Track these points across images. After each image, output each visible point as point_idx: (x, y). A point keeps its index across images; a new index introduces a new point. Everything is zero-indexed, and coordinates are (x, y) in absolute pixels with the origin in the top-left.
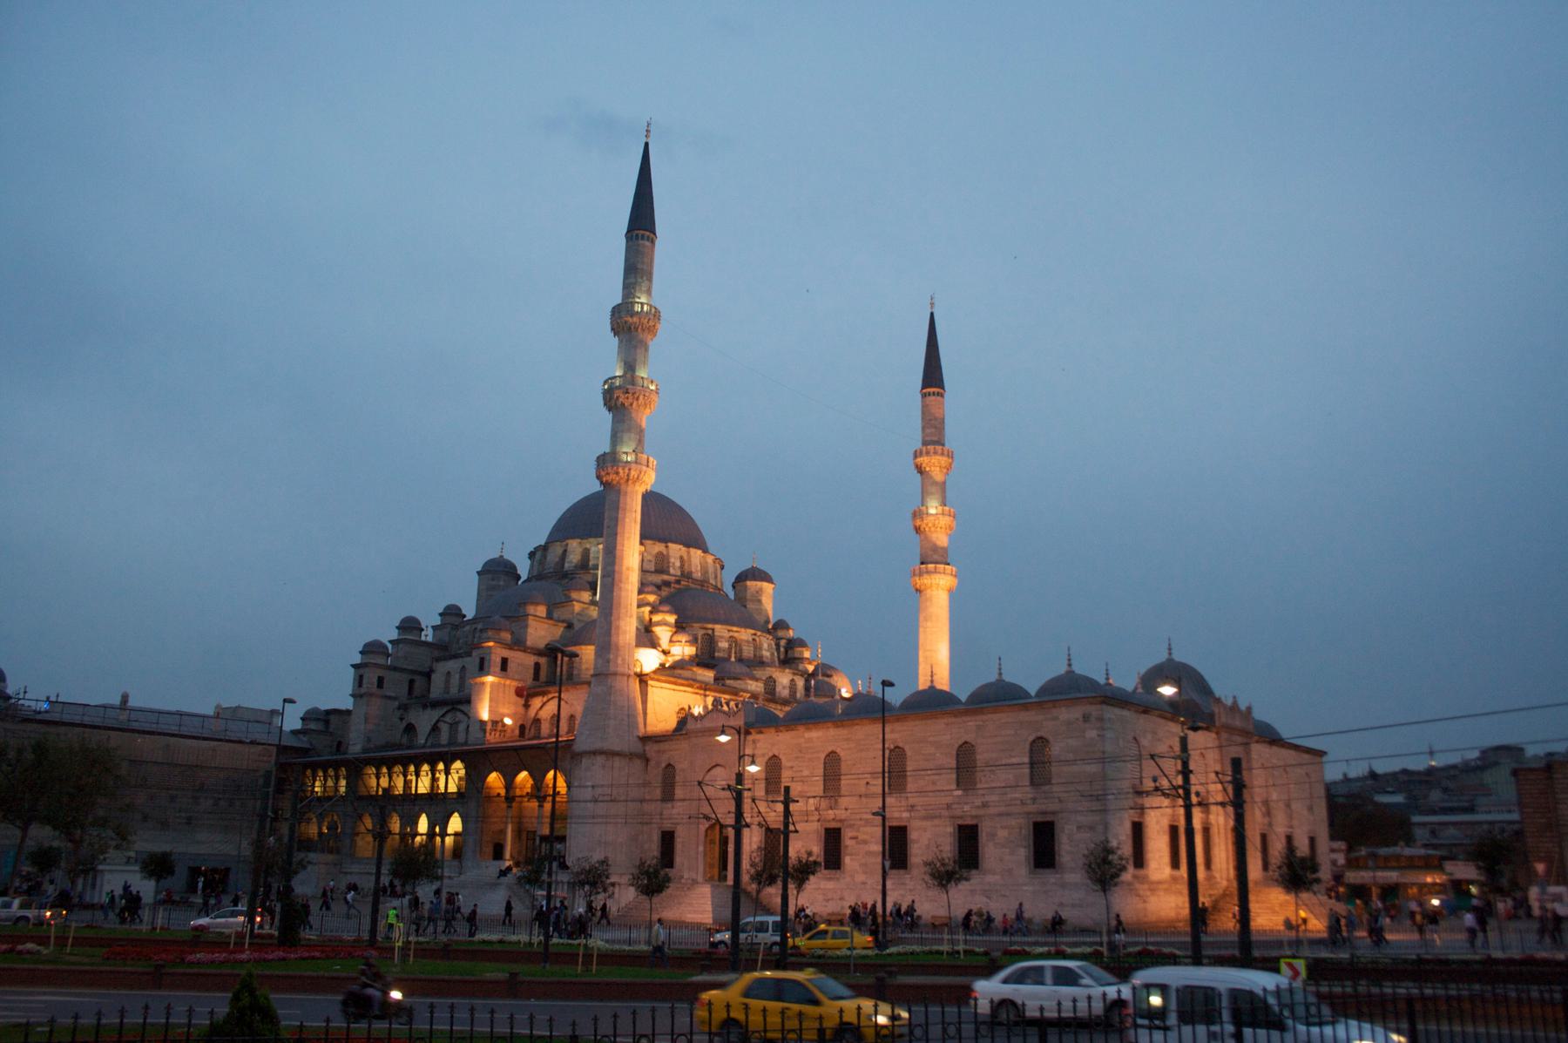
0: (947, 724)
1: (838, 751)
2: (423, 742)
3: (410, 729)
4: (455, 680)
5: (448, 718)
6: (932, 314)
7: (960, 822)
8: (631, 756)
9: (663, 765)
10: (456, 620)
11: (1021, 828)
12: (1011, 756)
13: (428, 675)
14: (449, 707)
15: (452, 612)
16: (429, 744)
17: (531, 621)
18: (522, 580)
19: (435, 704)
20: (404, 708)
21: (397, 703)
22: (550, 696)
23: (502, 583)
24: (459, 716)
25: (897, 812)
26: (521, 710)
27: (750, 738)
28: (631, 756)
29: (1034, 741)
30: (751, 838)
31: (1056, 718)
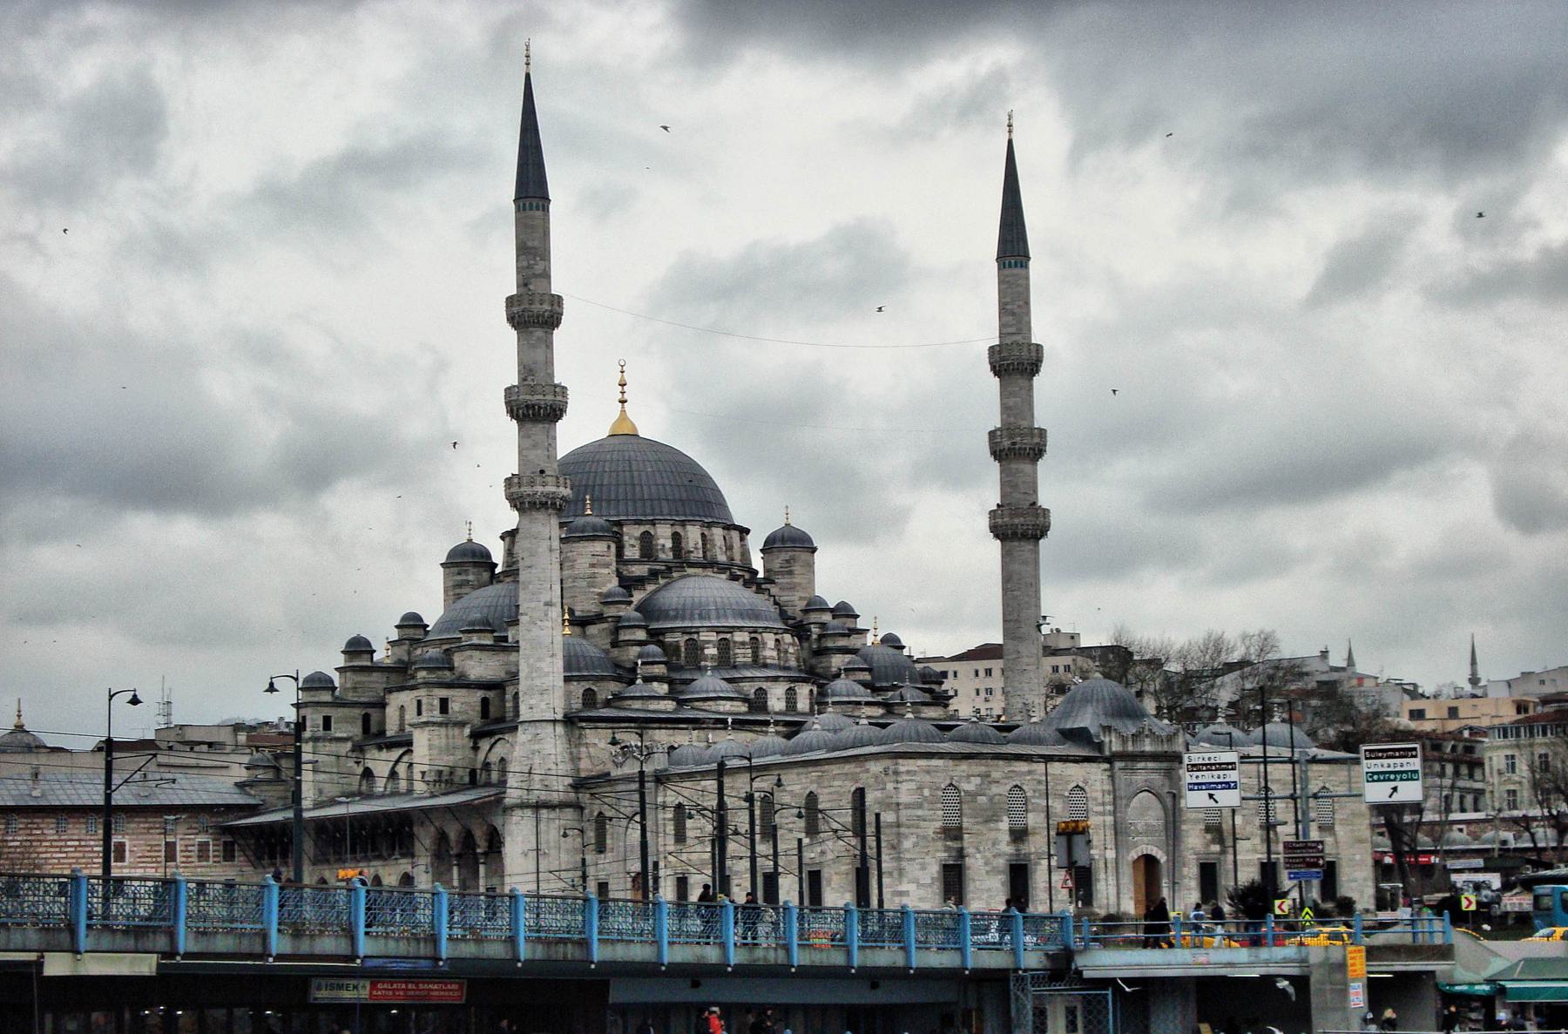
2: (382, 789)
3: (368, 774)
5: (405, 759)
8: (562, 805)
9: (595, 814)
10: (418, 634)
13: (382, 705)
15: (412, 624)
19: (391, 746)
20: (359, 748)
21: (349, 745)
22: (497, 737)
23: (471, 577)
26: (470, 754)
28: (562, 805)
31: (867, 771)
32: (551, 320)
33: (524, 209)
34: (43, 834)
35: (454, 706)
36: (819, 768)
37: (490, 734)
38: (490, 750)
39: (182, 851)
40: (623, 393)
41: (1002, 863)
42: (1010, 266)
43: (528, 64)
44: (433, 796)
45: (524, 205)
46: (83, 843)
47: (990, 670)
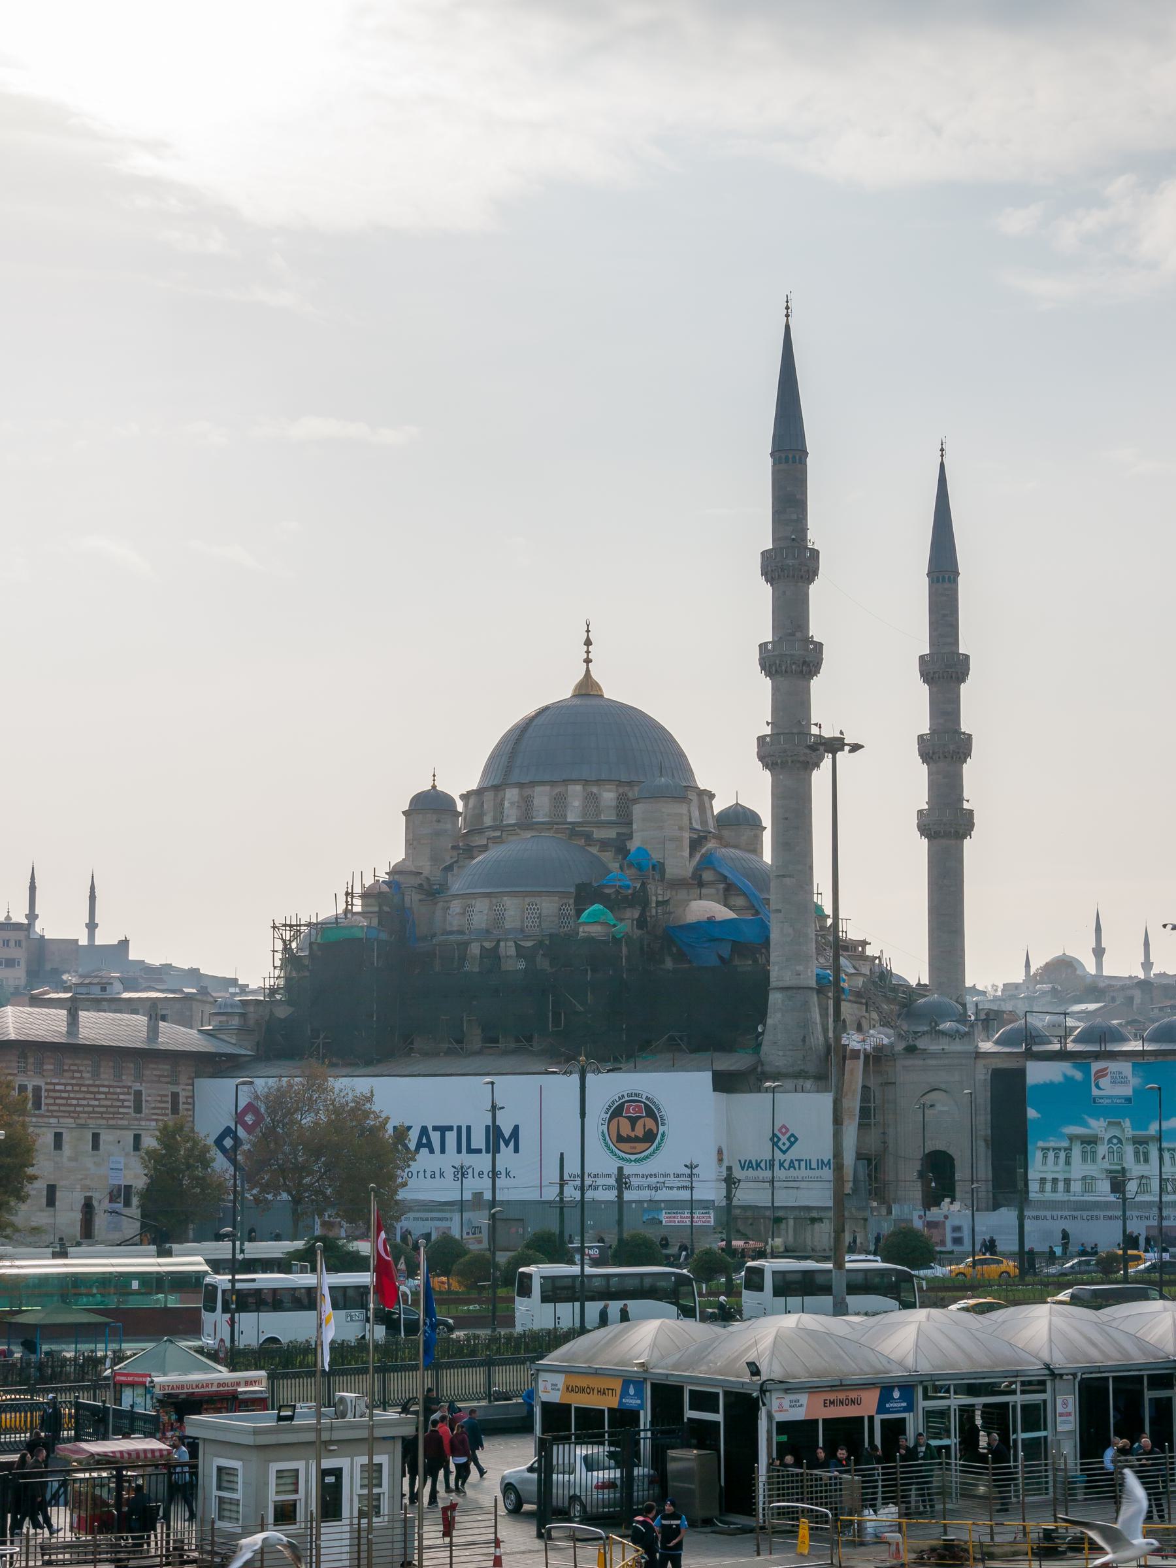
6: (942, 465)
39: (184, 1103)
42: (949, 581)
46: (111, 1090)
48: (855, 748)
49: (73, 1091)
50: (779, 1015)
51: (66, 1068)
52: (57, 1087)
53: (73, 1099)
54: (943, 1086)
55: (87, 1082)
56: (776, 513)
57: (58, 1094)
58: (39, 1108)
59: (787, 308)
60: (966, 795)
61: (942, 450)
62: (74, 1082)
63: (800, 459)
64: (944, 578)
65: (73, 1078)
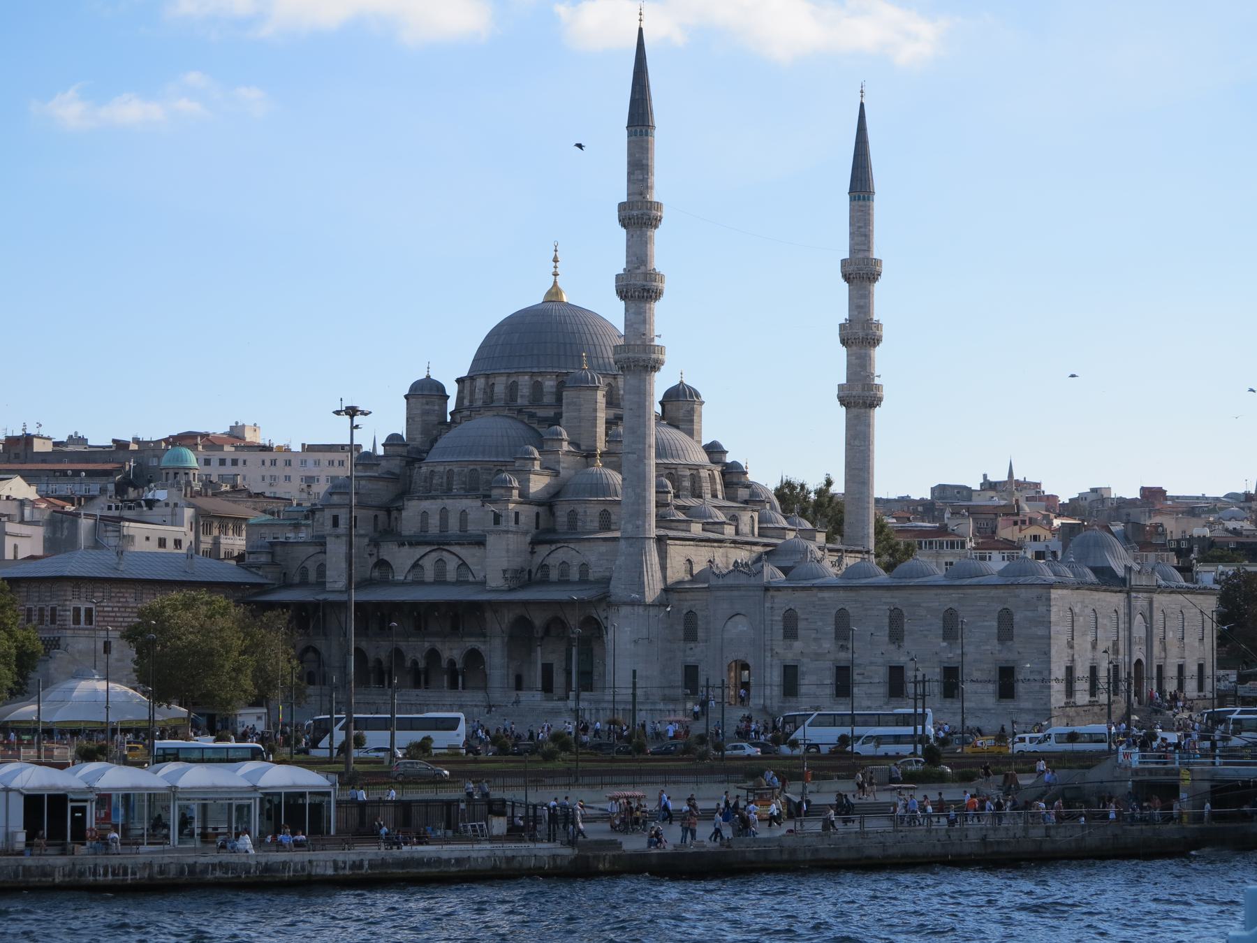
0: (936, 595)
1: (847, 608)
2: (402, 578)
3: (382, 564)
4: (434, 522)
5: (434, 555)
6: (862, 105)
7: (946, 665)
9: (685, 612)
11: (990, 671)
12: (984, 621)
14: (436, 547)
16: (410, 578)
17: (532, 476)
18: (451, 405)
19: (414, 542)
20: (375, 543)
21: (366, 540)
22: (559, 545)
24: (445, 554)
25: (901, 659)
27: (771, 593)
29: (1001, 611)
30: (771, 673)
32: (654, 222)
33: (641, 135)
34: (127, 601)
35: (522, 518)
36: (960, 591)
37: (551, 542)
38: (550, 554)
40: (556, 267)
41: (1088, 665)
42: (864, 199)
43: (641, 20)
44: (510, 590)
45: (641, 131)
47: (275, 460)
48: (363, 413)
49: (119, 611)
50: (623, 558)
51: (113, 595)
52: (106, 609)
53: (119, 617)
54: (743, 612)
55: (131, 605)
56: (630, 174)
57: (107, 614)
58: (91, 623)
59: (640, 14)
60: (877, 371)
61: (862, 92)
62: (120, 605)
63: (647, 131)
64: (859, 197)
65: (119, 602)
